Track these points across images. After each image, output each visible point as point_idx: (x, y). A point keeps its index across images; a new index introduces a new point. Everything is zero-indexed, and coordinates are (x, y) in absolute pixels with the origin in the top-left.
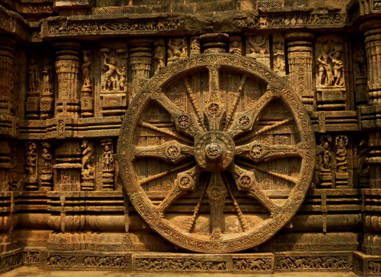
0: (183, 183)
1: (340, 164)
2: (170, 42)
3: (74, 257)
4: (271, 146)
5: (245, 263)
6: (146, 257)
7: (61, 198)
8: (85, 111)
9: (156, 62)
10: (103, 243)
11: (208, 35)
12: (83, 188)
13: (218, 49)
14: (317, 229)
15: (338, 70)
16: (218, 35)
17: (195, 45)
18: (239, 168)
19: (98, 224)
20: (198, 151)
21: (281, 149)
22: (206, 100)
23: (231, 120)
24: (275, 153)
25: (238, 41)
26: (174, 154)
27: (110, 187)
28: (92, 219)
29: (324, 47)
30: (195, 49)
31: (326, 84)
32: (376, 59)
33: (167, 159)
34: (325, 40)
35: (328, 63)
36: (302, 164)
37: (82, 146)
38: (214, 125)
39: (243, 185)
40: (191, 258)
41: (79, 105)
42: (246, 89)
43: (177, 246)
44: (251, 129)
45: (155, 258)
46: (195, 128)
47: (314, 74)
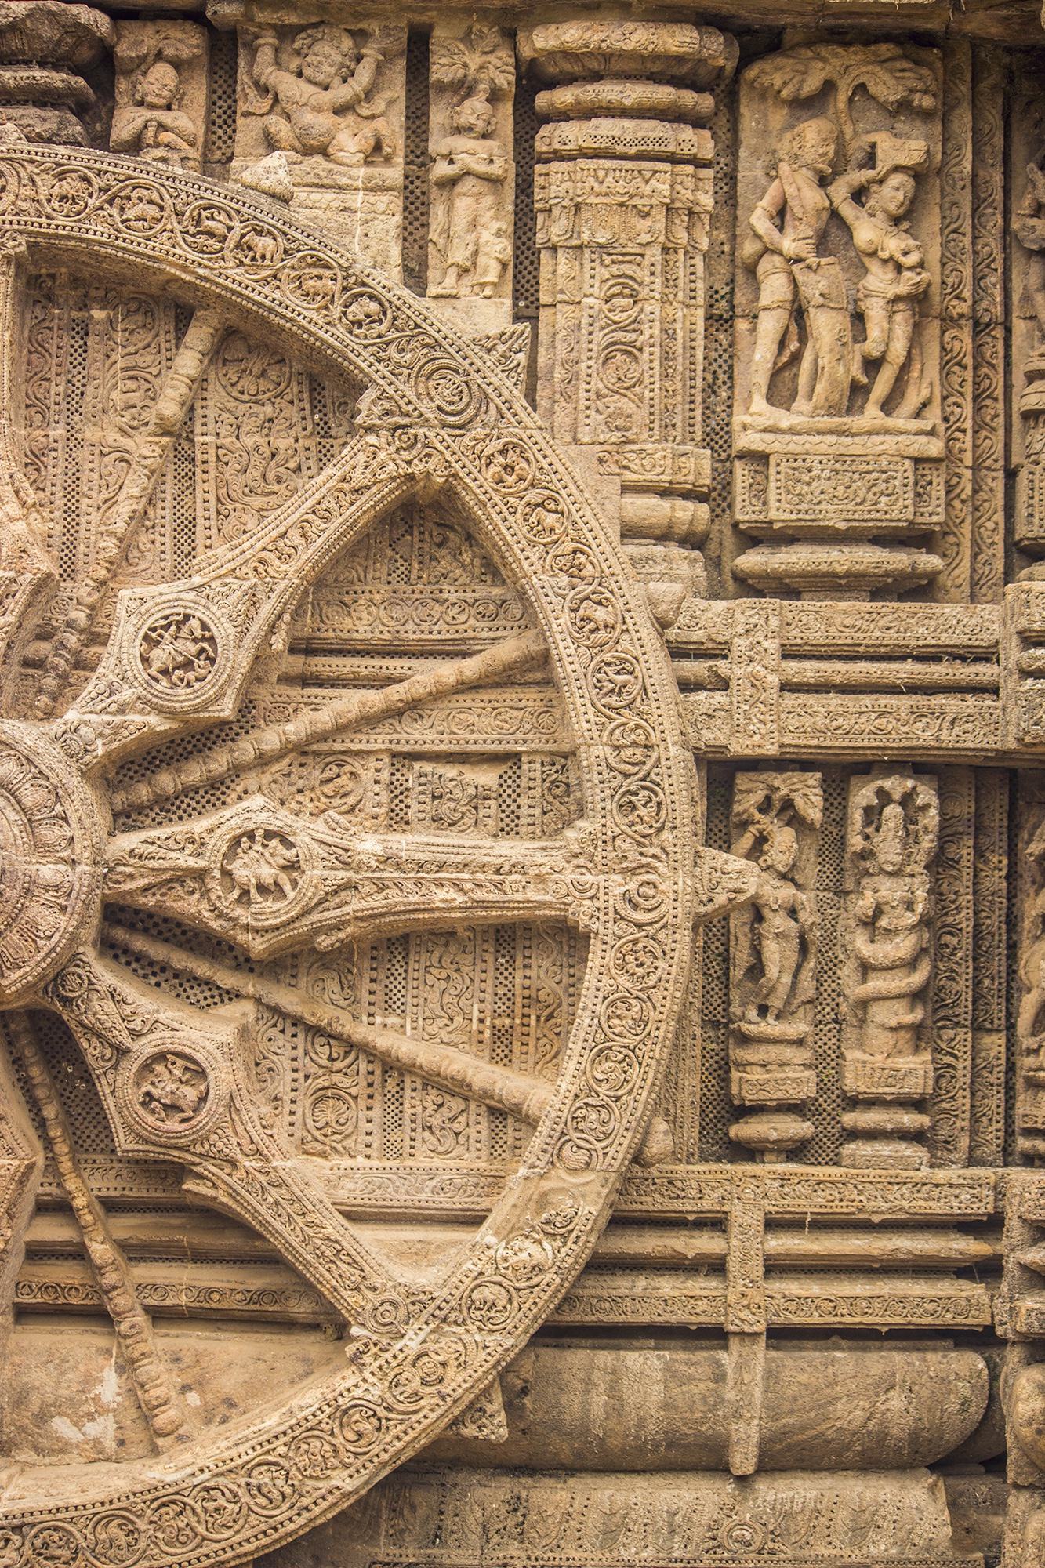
1: (877, 984)
4: (369, 845)
13: (30, 114)
16: (30, 15)
18: (129, 989)
21: (441, 866)
23: (96, 638)
24: (394, 897)
25: (177, 64)
31: (801, 404)
34: (812, 84)
36: (590, 979)
42: (212, 413)
44: (227, 709)
47: (720, 320)
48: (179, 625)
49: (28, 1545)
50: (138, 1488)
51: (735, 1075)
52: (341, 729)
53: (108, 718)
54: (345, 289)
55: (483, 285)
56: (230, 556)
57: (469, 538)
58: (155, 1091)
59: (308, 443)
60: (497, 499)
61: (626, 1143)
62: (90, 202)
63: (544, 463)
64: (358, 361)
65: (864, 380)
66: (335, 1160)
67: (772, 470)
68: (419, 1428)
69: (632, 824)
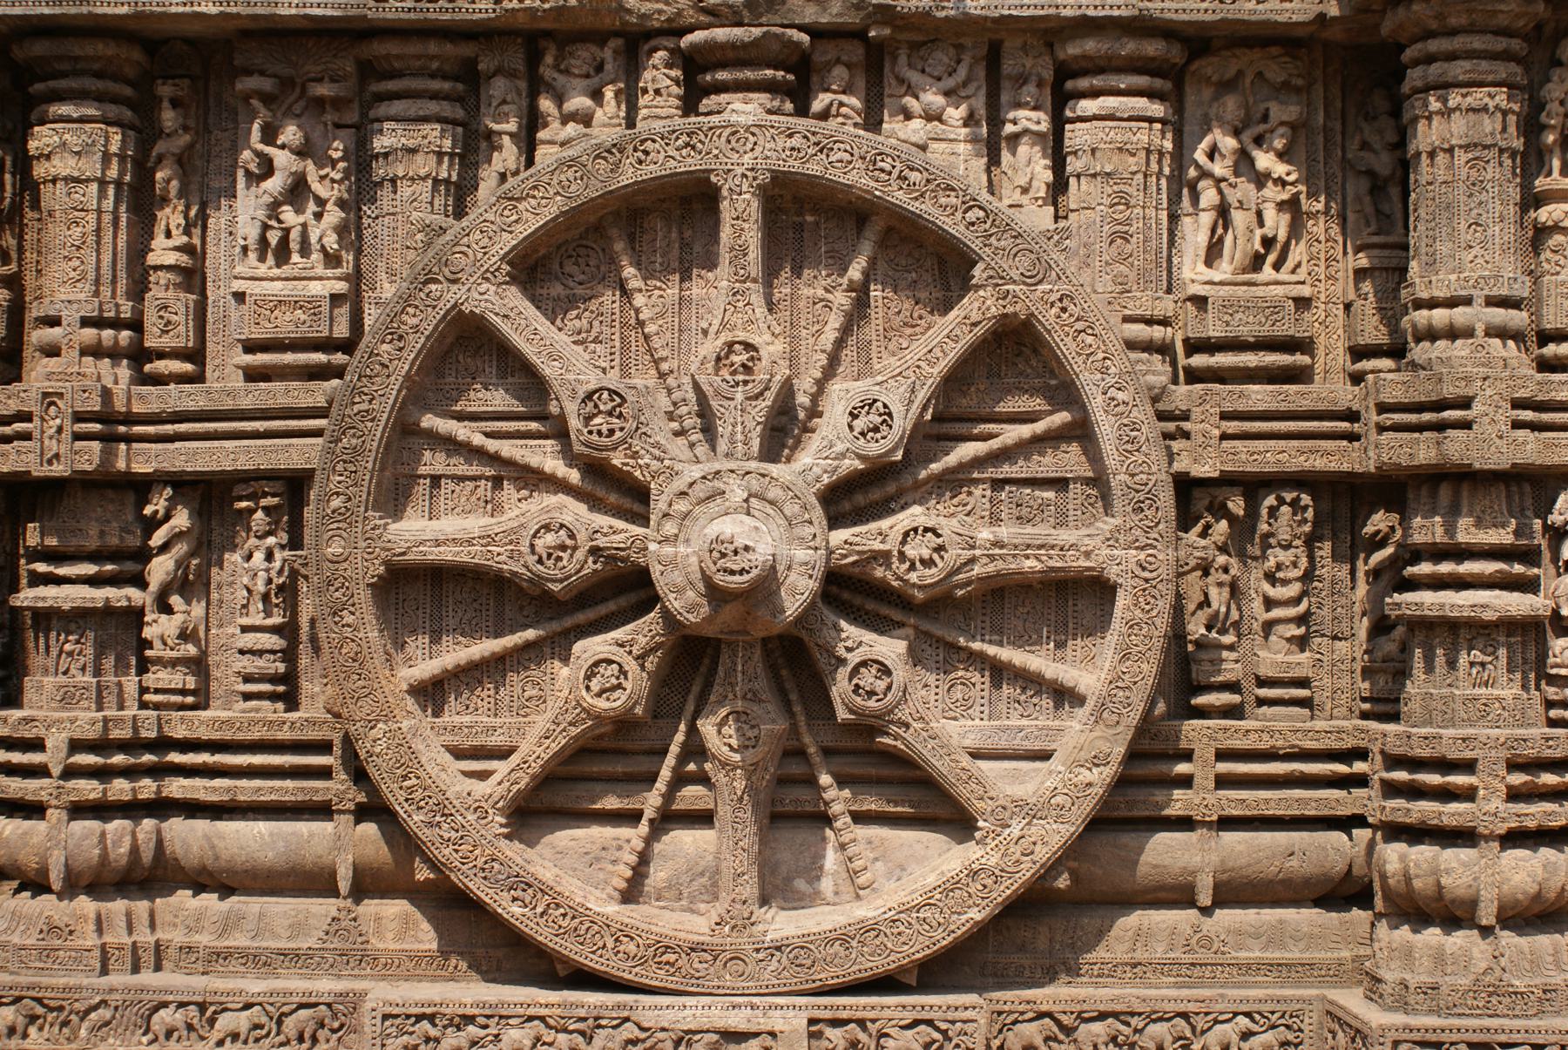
0: (595, 685)
1: (1277, 613)
2: (549, 59)
3: (104, 1003)
4: (985, 534)
5: (862, 1036)
6: (429, 1011)
7: (49, 744)
8: (161, 355)
9: (484, 145)
10: (239, 940)
11: (721, 34)
12: (147, 697)
13: (763, 97)
14: (1179, 895)
15: (1281, 206)
16: (765, 34)
17: (659, 75)
19: (217, 858)
20: (668, 550)
21: (1028, 546)
22: (704, 325)
23: (814, 412)
24: (1000, 565)
25: (848, 66)
26: (559, 559)
27: (273, 697)
28: (187, 836)
29: (1224, 104)
30: (657, 92)
32: (1450, 167)
33: (530, 581)
34: (1231, 72)
35: (1237, 174)
37: (148, 510)
38: (739, 437)
39: (859, 699)
40: (626, 1014)
41: (137, 325)
43: (565, 961)
44: (899, 456)
45: (470, 1011)
46: (657, 445)
48: (871, 405)
49: (785, 956)
50: (852, 921)
51: (1194, 668)
52: (962, 467)
53: (830, 462)
54: (964, 203)
55: (1037, 199)
56: (898, 363)
57: (1035, 351)
58: (862, 683)
59: (939, 295)
60: (1057, 328)
61: (1141, 709)
62: (809, 151)
63: (1085, 306)
64: (973, 246)
65: (1262, 251)
66: (962, 722)
67: (1210, 307)
68: (1020, 881)
69: (1141, 520)
